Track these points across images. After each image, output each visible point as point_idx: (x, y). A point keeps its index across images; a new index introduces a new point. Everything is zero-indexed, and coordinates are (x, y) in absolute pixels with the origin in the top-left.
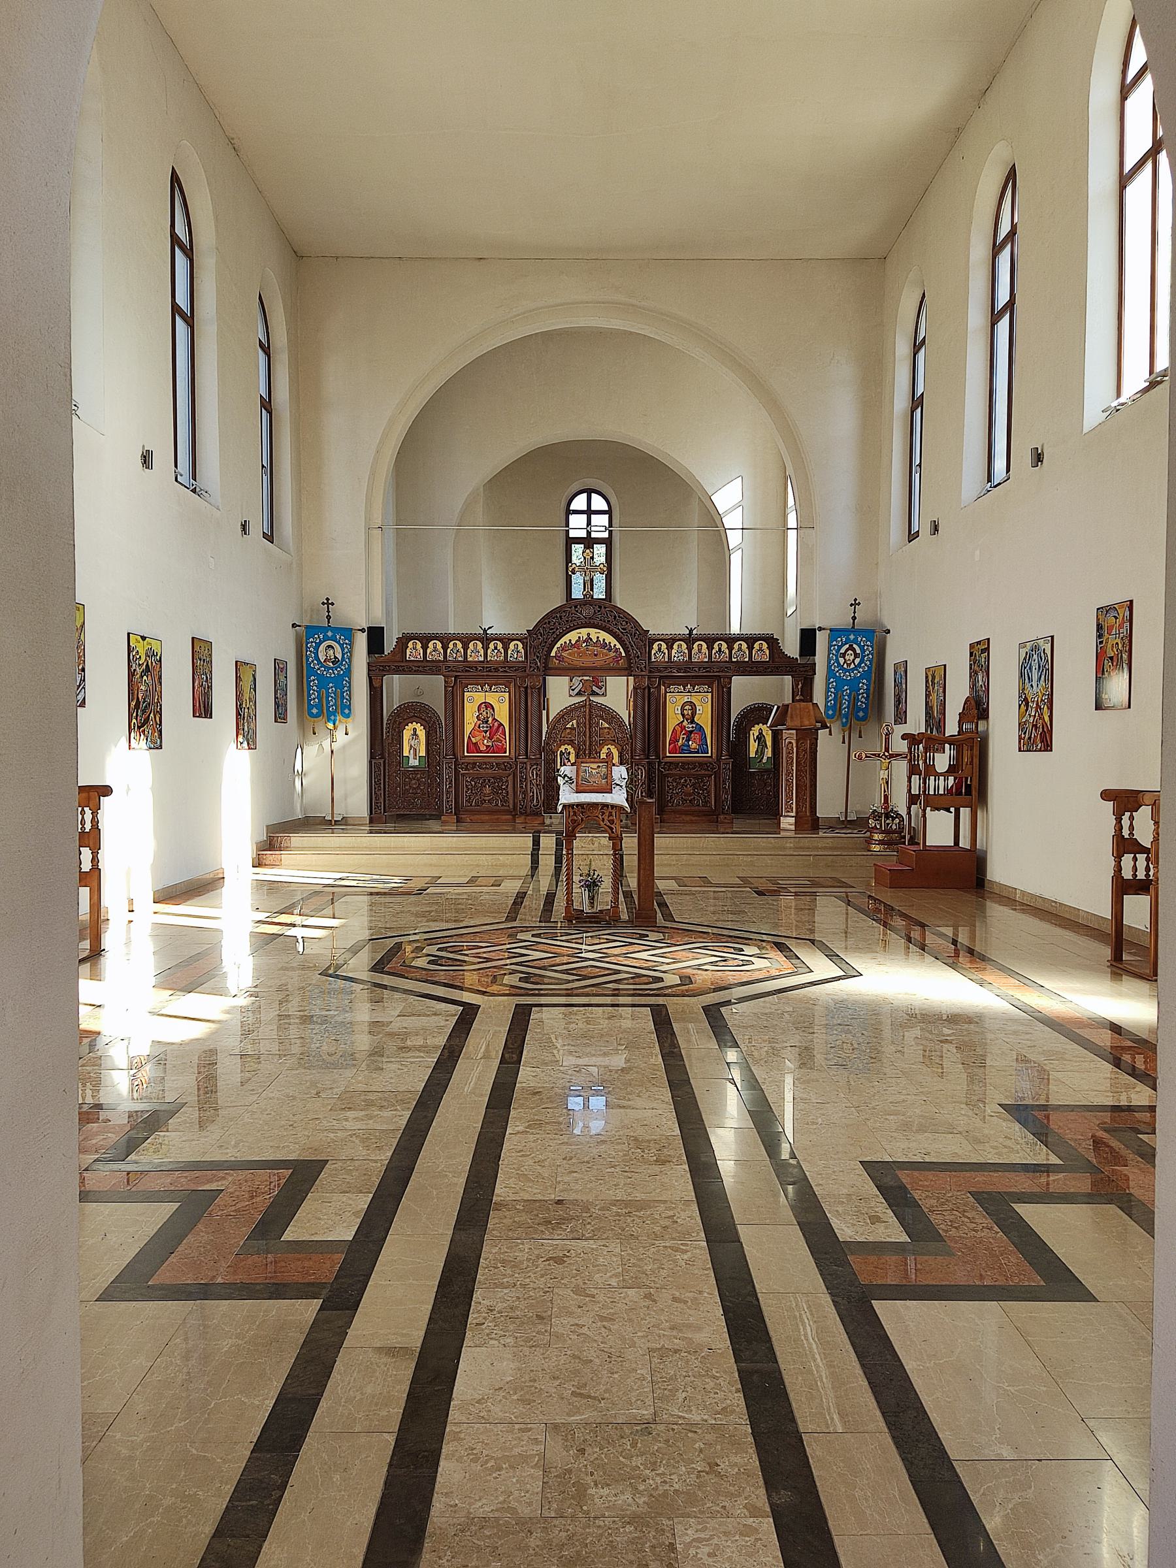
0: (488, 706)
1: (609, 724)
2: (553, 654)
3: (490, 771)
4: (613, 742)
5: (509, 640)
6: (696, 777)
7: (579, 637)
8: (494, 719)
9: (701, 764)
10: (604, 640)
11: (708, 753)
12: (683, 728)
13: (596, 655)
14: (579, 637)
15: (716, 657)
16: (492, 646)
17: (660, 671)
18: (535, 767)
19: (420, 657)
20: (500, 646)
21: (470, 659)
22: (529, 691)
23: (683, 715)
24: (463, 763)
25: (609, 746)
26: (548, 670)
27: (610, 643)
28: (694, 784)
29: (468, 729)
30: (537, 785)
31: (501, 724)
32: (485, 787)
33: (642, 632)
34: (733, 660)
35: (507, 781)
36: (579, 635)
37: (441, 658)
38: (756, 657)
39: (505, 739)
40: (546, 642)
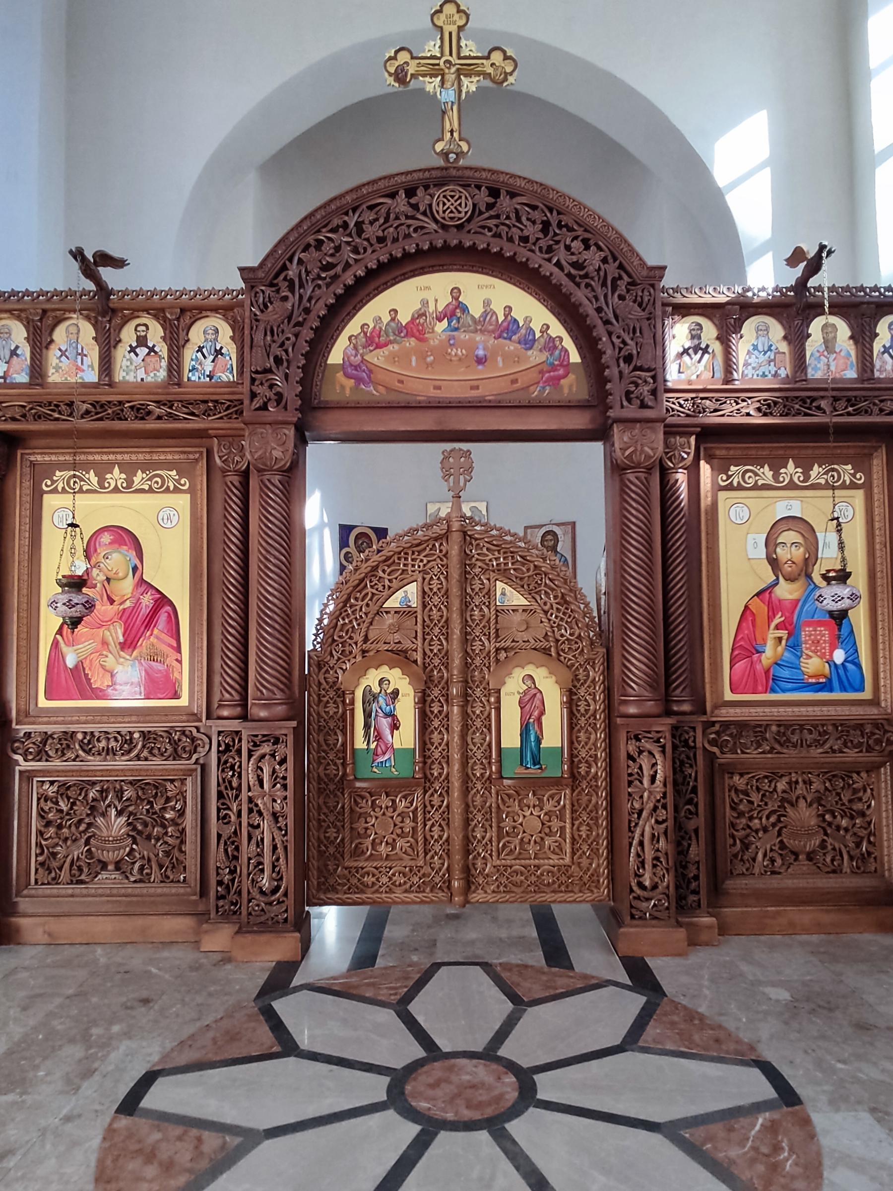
1: (531, 592)
2: (336, 357)
3: (121, 763)
5: (183, 311)
6: (831, 773)
7: (425, 303)
8: (142, 581)
11: (862, 689)
12: (773, 607)
13: (480, 361)
14: (425, 303)
16: (128, 335)
18: (266, 749)
20: (156, 333)
21: (54, 377)
22: (254, 483)
23: (774, 563)
24: (28, 735)
25: (530, 670)
27: (528, 320)
28: (819, 800)
30: (275, 816)
31: (162, 601)
32: (104, 815)
33: (640, 274)
35: (182, 794)
36: (425, 295)
39: (178, 649)
40: (307, 311)
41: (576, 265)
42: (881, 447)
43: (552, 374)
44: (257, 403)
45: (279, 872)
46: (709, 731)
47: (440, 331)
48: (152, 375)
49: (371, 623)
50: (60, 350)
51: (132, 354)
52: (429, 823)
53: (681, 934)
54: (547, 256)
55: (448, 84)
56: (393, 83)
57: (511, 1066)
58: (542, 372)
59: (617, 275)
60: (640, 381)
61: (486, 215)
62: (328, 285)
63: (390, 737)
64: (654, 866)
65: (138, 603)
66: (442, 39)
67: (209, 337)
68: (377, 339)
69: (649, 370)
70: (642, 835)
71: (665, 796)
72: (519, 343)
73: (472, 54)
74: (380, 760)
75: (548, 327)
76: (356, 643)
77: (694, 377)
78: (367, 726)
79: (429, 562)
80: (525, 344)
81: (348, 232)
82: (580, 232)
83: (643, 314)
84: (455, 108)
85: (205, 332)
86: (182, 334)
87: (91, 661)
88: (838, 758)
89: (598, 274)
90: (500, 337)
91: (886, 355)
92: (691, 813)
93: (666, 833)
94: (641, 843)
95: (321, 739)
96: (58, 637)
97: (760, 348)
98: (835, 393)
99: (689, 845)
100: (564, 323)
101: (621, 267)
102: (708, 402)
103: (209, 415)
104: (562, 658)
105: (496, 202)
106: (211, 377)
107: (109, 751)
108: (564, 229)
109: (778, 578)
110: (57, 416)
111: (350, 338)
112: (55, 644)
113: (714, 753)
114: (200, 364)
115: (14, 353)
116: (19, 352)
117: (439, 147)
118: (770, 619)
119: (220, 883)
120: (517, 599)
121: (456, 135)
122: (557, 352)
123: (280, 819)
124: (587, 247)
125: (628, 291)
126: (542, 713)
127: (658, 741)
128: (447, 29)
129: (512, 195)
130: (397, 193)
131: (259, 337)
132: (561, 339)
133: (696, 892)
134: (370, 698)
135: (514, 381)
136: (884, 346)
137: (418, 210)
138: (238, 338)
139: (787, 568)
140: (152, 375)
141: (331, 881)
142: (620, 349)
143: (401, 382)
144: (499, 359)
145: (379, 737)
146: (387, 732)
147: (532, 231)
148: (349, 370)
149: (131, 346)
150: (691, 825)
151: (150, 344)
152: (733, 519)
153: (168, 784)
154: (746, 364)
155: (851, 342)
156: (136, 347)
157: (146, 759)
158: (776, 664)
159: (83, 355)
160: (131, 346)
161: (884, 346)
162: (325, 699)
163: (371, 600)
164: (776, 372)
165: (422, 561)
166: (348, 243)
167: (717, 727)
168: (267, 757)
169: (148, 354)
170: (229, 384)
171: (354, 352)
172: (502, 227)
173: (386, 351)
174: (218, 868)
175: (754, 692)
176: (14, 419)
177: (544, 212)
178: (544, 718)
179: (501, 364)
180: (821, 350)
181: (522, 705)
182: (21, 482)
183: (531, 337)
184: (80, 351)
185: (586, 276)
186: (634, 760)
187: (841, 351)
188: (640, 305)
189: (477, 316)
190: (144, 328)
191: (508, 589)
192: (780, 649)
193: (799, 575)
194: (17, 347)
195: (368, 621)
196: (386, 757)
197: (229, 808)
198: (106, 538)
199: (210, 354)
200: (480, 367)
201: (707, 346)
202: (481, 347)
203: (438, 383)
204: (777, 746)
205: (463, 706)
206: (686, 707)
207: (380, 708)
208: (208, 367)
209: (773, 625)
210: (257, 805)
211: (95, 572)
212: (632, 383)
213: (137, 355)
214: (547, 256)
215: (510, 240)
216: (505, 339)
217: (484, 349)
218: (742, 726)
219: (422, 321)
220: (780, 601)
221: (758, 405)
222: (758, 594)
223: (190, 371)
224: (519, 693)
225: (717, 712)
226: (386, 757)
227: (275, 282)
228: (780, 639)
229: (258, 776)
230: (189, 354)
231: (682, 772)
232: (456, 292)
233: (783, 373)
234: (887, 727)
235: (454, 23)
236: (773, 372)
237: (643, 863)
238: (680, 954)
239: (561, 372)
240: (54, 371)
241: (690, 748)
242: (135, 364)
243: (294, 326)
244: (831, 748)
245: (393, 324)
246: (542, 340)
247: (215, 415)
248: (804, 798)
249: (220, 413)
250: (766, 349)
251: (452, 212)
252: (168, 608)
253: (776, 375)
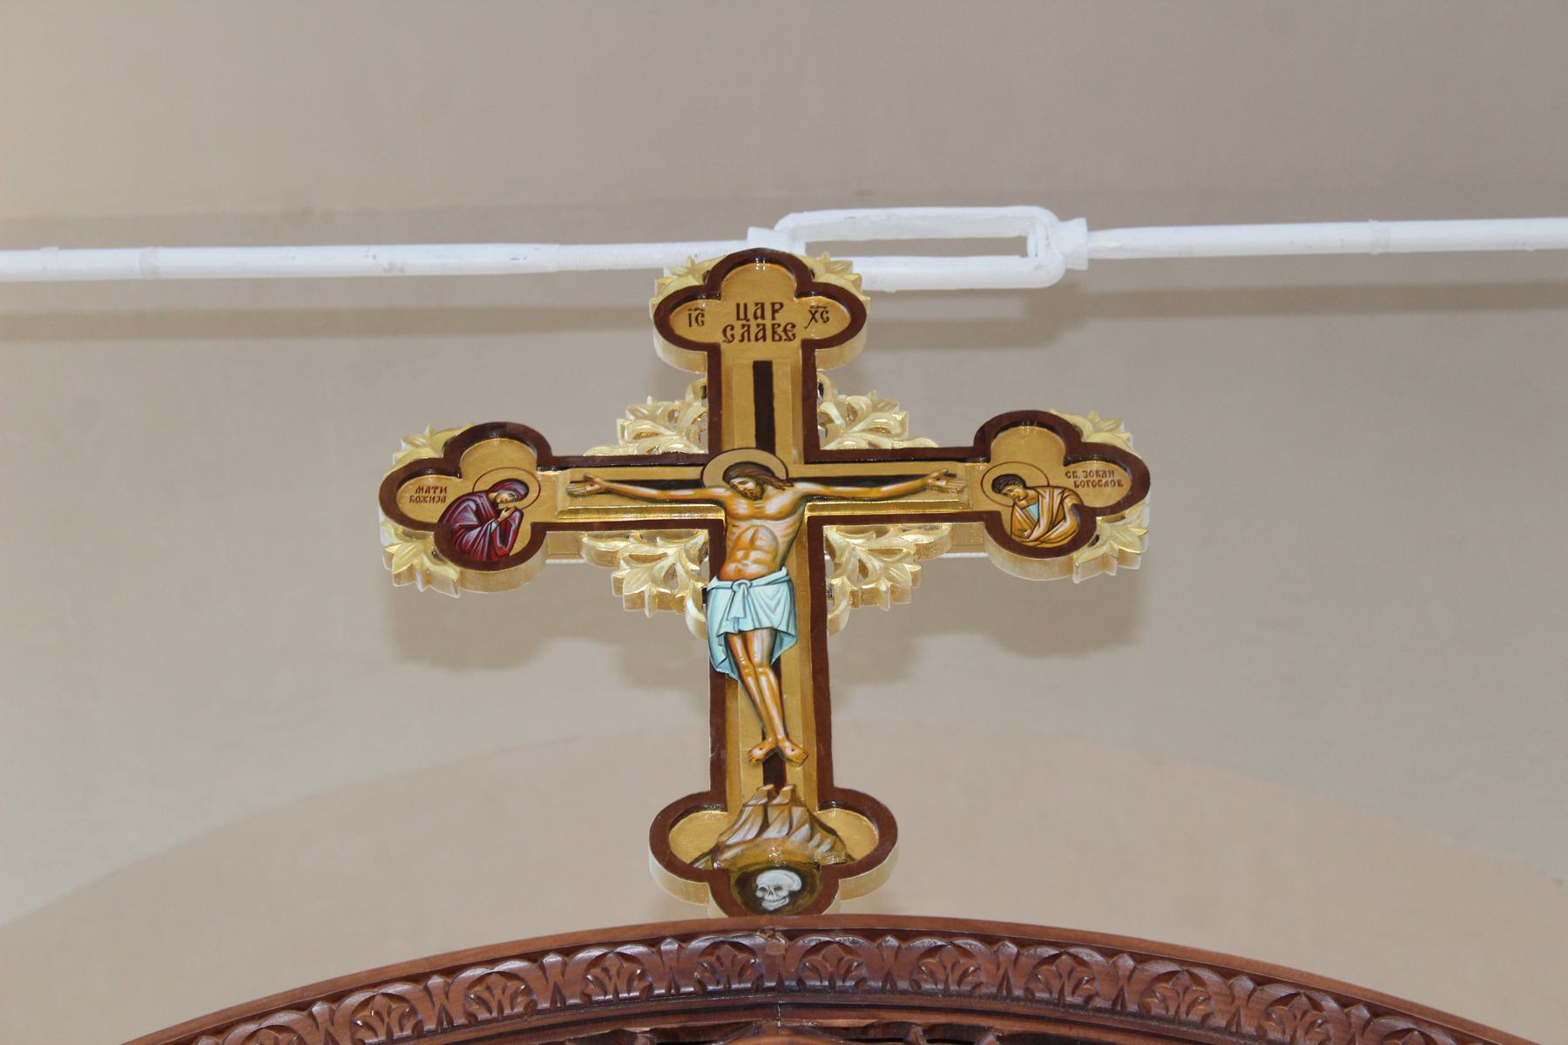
56: (428, 563)
66: (714, 393)
73: (887, 443)
117: (691, 839)
128: (739, 360)
235: (788, 333)
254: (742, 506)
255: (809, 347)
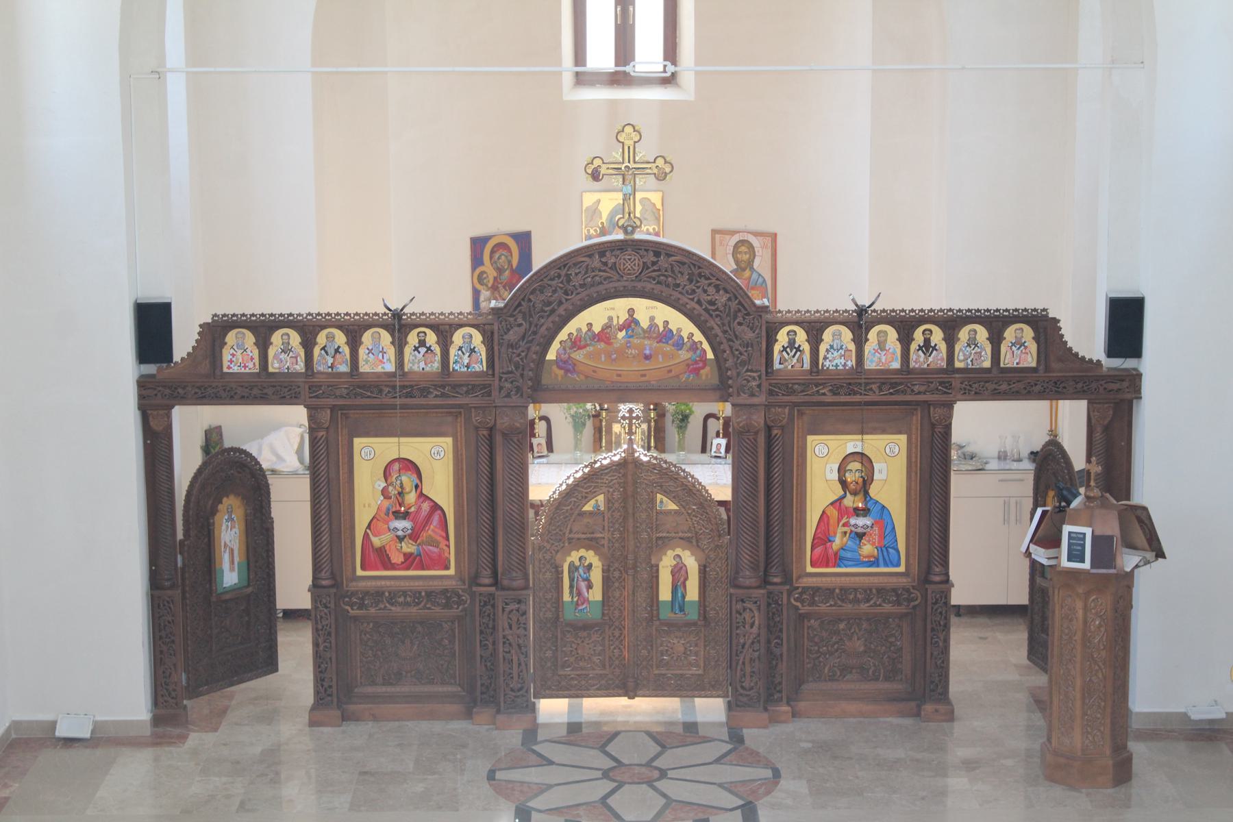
0: (409, 466)
2: (551, 355)
3: (414, 610)
4: (691, 541)
5: (450, 325)
7: (610, 319)
9: (881, 591)
10: (666, 323)
13: (647, 357)
14: (610, 319)
15: (918, 359)
16: (413, 338)
17: (792, 392)
19: (253, 367)
20: (431, 338)
21: (364, 368)
22: (499, 439)
23: (843, 483)
25: (678, 551)
26: (539, 391)
27: (679, 330)
29: (362, 518)
30: (519, 646)
31: (436, 507)
34: (958, 365)
37: (300, 367)
38: (1009, 359)
39: (447, 539)
40: (535, 333)
41: (712, 303)
42: (916, 409)
43: (695, 366)
44: (503, 393)
45: (522, 679)
46: (794, 592)
47: (620, 338)
48: (429, 365)
49: (574, 521)
50: (368, 349)
51: (416, 352)
52: (612, 647)
53: (765, 716)
54: (691, 297)
55: (627, 182)
57: (656, 768)
58: (688, 365)
59: (737, 309)
60: (750, 379)
61: (652, 269)
62: (548, 316)
63: (586, 594)
64: (751, 676)
65: (419, 508)
67: (466, 340)
68: (578, 343)
69: (756, 372)
70: (744, 659)
71: (759, 635)
72: (673, 345)
74: (580, 608)
75: (693, 335)
76: (564, 534)
77: (790, 367)
78: (571, 587)
79: (612, 480)
80: (678, 346)
81: (560, 280)
82: (714, 280)
83: (753, 335)
84: (631, 197)
85: (463, 337)
86: (449, 339)
87: (390, 546)
88: (878, 610)
89: (725, 308)
90: (660, 341)
91: (920, 352)
92: (779, 644)
93: (759, 658)
94: (744, 663)
95: (541, 594)
96: (368, 531)
97: (835, 347)
98: (882, 381)
99: (777, 664)
100: (703, 333)
101: (740, 303)
102: (796, 386)
103: (469, 394)
104: (700, 544)
105: (658, 261)
106: (468, 366)
107: (407, 604)
108: (703, 278)
109: (846, 493)
110: (369, 394)
111: (560, 343)
112: (366, 536)
113: (798, 606)
114: (461, 358)
115: (337, 351)
116: (340, 350)
118: (839, 520)
119: (482, 685)
120: (672, 506)
121: (632, 215)
122: (698, 352)
123: (522, 648)
124: (718, 291)
125: (744, 319)
126: (686, 579)
127: (756, 603)
129: (669, 255)
130: (593, 254)
131: (503, 350)
132: (701, 343)
133: (780, 691)
134: (573, 569)
135: (670, 371)
136: (919, 346)
137: (607, 266)
138: (489, 340)
139: (852, 487)
140: (429, 365)
141: (549, 683)
142: (738, 358)
143: (594, 371)
144: (660, 356)
145: (579, 594)
146: (584, 590)
147: (682, 280)
148: (560, 364)
149: (415, 346)
150: (777, 651)
151: (428, 345)
152: (817, 454)
153: (443, 623)
154: (825, 358)
155: (898, 343)
156: (419, 347)
157: (429, 609)
158: (842, 549)
159: (383, 353)
160: (415, 346)
161: (919, 346)
162: (543, 570)
163: (574, 505)
164: (845, 363)
165: (607, 480)
166: (561, 288)
167: (800, 590)
168: (514, 612)
169: (426, 352)
170: (481, 374)
171: (563, 352)
172: (662, 278)
173: (584, 351)
174: (481, 676)
175: (827, 566)
176: (342, 397)
177: (690, 267)
178: (687, 583)
179: (661, 360)
180: (876, 348)
181: (673, 573)
182: (342, 433)
183: (681, 342)
184: (381, 349)
185: (717, 309)
186: (740, 614)
187: (890, 349)
188: (751, 329)
189: (645, 327)
190: (423, 334)
191: (665, 499)
192: (845, 539)
193: (860, 491)
194: (339, 347)
195: (572, 520)
196: (584, 607)
197: (487, 640)
198: (396, 466)
199: (467, 352)
200: (647, 362)
201: (800, 346)
202: (648, 348)
203: (619, 372)
204: (839, 603)
205: (634, 575)
206: (776, 580)
207: (580, 576)
208: (466, 361)
209: (841, 524)
210: (508, 640)
211: (390, 488)
212: (745, 379)
213: (419, 352)
214: (691, 297)
215: (668, 286)
216: (664, 343)
217: (650, 350)
218: (816, 590)
219: (608, 331)
220: (846, 508)
221: (831, 388)
222: (832, 504)
223: (454, 363)
224: (671, 566)
225: (800, 580)
226: (584, 607)
227: (514, 313)
228: (845, 533)
229: (509, 623)
230: (453, 351)
231: (773, 618)
232: (631, 311)
233: (849, 364)
234: (912, 590)
236: (843, 364)
237: (744, 675)
238: (765, 727)
239: (701, 365)
240: (364, 363)
241: (779, 605)
242: (418, 359)
243: (526, 343)
244: (875, 603)
245: (589, 333)
246: (689, 344)
247: (472, 394)
248: (857, 634)
249: (476, 392)
250: (839, 348)
251: (629, 270)
252: (439, 512)
253: (845, 365)
254: (626, 173)
255: (635, 142)
